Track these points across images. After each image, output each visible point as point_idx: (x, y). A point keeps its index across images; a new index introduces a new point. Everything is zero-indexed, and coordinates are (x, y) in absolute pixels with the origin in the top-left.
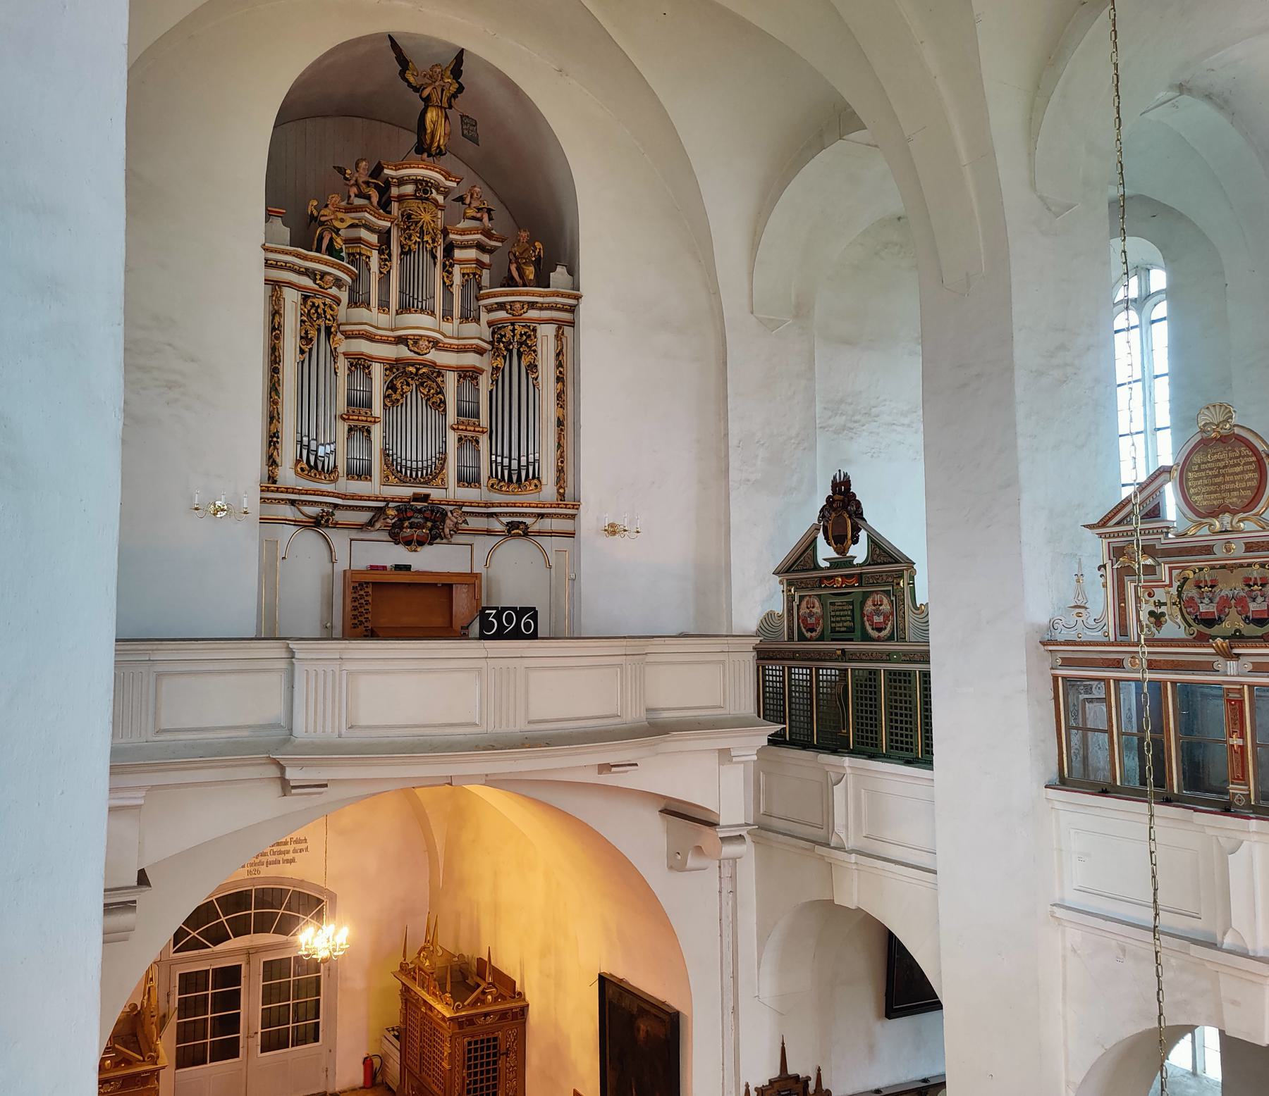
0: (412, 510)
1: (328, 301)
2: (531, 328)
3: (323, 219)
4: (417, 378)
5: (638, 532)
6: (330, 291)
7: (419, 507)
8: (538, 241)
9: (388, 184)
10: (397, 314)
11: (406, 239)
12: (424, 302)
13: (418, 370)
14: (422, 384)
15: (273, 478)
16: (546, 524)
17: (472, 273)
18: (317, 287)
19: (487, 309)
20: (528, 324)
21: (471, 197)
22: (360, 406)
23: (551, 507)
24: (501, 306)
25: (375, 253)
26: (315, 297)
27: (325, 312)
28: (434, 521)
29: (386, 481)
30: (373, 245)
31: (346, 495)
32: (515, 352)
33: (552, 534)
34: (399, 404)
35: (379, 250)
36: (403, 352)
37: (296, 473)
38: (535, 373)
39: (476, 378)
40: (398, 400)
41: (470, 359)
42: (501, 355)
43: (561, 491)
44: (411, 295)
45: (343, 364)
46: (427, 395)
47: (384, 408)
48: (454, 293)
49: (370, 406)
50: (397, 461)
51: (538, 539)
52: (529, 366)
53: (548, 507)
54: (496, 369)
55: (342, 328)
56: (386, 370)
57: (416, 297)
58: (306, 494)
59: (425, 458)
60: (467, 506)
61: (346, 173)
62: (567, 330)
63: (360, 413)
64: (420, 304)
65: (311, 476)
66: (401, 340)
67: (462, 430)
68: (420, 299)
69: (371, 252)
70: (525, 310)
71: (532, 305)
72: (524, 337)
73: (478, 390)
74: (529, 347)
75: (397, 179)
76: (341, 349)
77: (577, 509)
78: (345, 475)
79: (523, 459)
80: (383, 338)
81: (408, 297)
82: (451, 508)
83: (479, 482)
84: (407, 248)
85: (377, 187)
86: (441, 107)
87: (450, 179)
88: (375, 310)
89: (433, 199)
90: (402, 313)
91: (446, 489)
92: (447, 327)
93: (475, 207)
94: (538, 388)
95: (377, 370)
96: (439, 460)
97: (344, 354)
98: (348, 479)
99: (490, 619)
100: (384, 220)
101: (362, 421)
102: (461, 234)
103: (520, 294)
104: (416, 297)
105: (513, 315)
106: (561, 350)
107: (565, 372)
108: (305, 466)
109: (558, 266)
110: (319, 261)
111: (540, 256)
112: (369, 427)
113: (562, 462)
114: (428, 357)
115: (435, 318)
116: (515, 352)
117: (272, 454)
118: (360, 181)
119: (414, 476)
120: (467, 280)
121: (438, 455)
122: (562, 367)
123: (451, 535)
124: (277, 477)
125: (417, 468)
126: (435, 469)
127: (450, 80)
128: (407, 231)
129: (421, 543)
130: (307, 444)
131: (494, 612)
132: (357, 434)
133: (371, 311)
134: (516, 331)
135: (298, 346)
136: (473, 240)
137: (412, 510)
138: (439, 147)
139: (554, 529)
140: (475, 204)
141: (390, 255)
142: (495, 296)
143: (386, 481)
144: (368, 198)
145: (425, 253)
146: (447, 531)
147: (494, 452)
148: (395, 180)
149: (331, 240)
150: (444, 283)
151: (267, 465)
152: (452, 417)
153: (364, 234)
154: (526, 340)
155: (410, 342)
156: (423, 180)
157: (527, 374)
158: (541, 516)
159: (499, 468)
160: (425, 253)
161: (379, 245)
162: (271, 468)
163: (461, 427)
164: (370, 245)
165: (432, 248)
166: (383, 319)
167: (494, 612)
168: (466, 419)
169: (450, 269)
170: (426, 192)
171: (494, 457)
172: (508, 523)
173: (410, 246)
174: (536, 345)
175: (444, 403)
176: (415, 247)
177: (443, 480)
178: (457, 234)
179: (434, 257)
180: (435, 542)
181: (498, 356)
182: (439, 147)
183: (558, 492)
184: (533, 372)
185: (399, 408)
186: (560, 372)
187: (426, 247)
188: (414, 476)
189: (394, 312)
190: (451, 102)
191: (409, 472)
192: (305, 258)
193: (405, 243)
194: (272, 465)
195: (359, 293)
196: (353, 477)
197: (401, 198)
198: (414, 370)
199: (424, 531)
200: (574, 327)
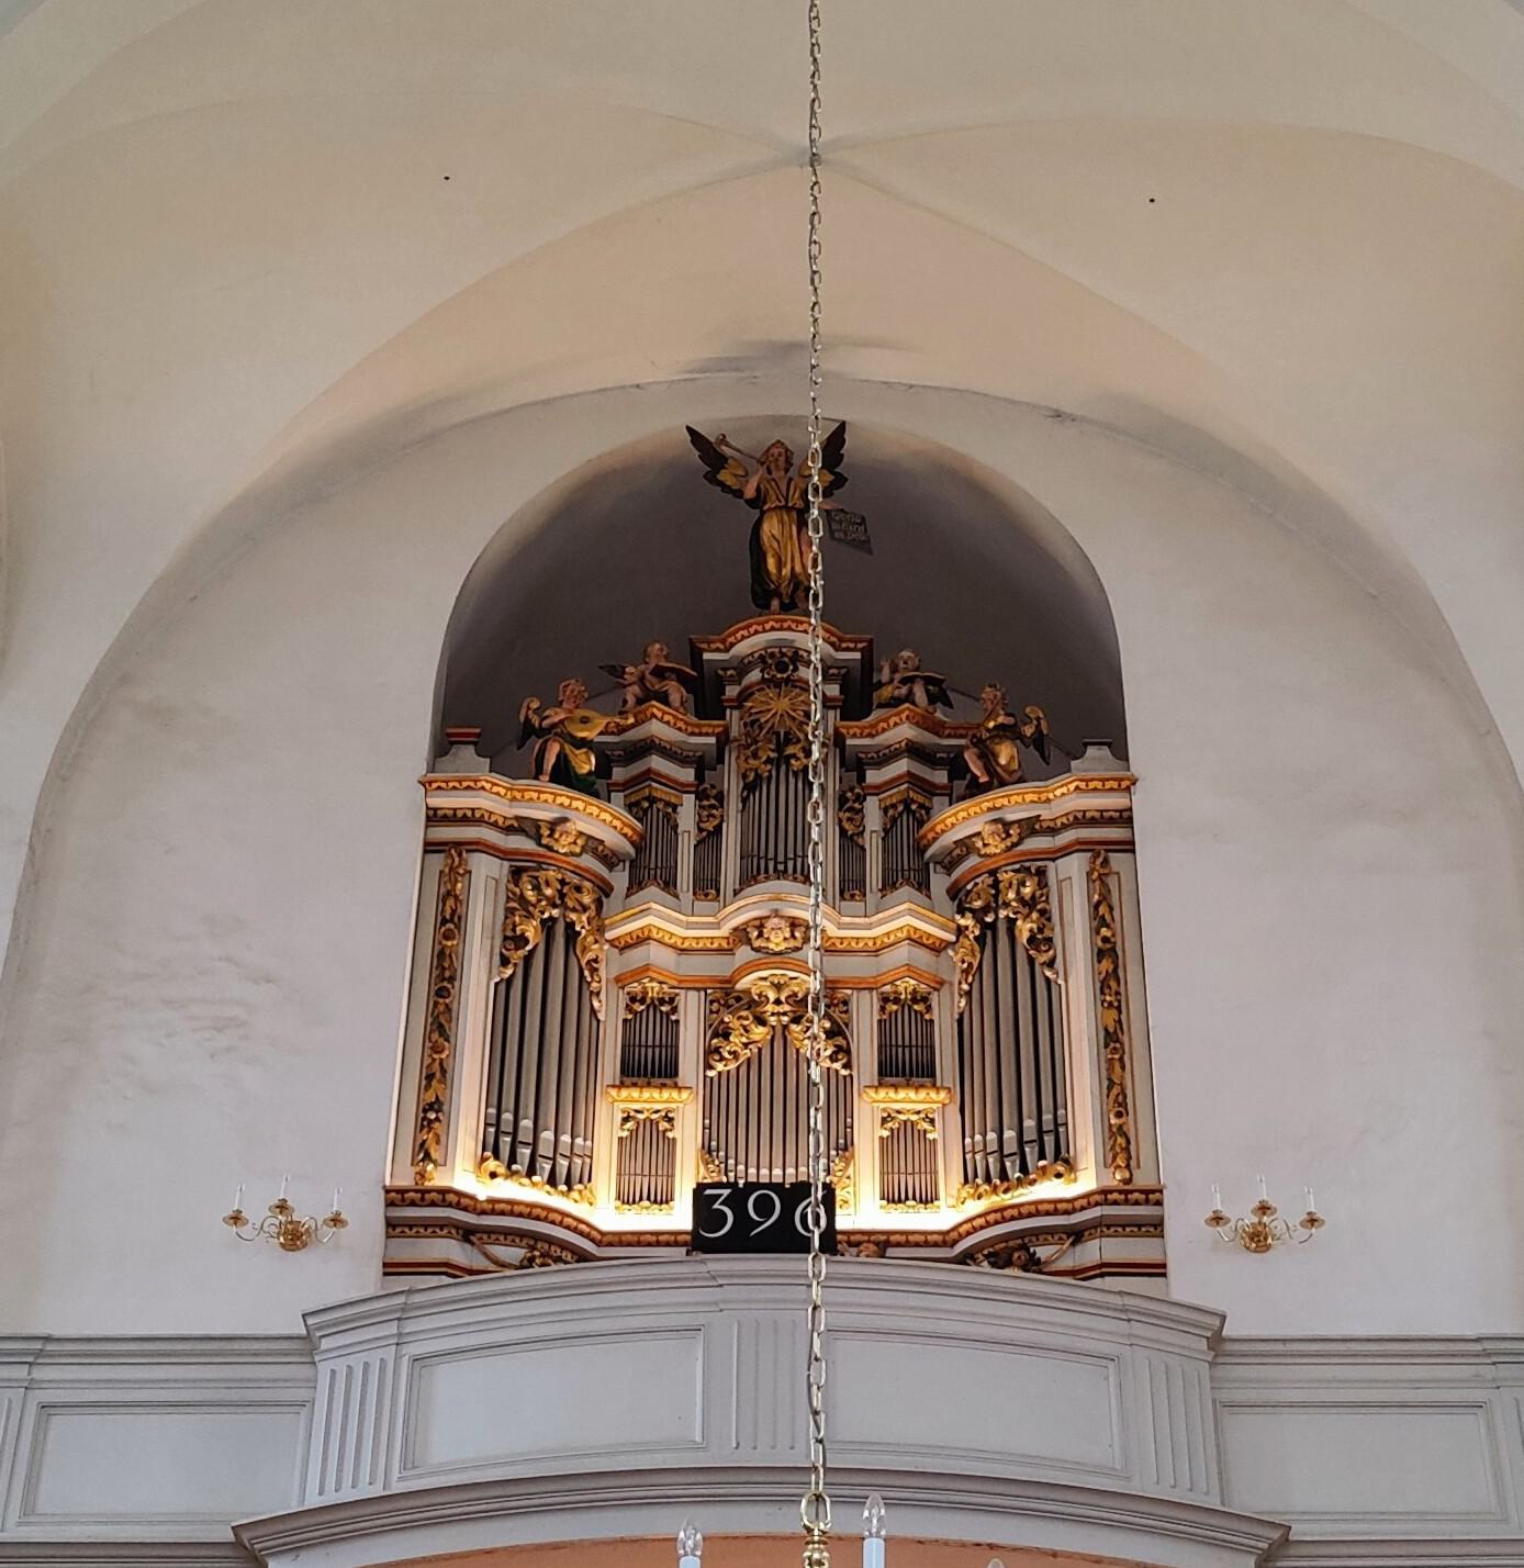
2: (1033, 871)
8: (1027, 705)
12: (790, 864)
17: (900, 802)
20: (1027, 864)
22: (645, 1075)
25: (689, 800)
30: (683, 785)
57: (771, 855)
60: (898, 1245)
64: (781, 867)
75: (734, 669)
79: (1029, 1123)
87: (844, 645)
89: (800, 680)
104: (771, 855)
109: (1089, 747)
111: (1041, 732)
133: (677, 897)
134: (1001, 885)
135: (497, 951)
141: (720, 798)
148: (729, 673)
150: (843, 832)
158: (1077, 1235)
164: (682, 788)
169: (857, 805)
174: (1047, 901)
175: (848, 1052)
178: (862, 736)
197: (745, 695)
200: (1133, 851)
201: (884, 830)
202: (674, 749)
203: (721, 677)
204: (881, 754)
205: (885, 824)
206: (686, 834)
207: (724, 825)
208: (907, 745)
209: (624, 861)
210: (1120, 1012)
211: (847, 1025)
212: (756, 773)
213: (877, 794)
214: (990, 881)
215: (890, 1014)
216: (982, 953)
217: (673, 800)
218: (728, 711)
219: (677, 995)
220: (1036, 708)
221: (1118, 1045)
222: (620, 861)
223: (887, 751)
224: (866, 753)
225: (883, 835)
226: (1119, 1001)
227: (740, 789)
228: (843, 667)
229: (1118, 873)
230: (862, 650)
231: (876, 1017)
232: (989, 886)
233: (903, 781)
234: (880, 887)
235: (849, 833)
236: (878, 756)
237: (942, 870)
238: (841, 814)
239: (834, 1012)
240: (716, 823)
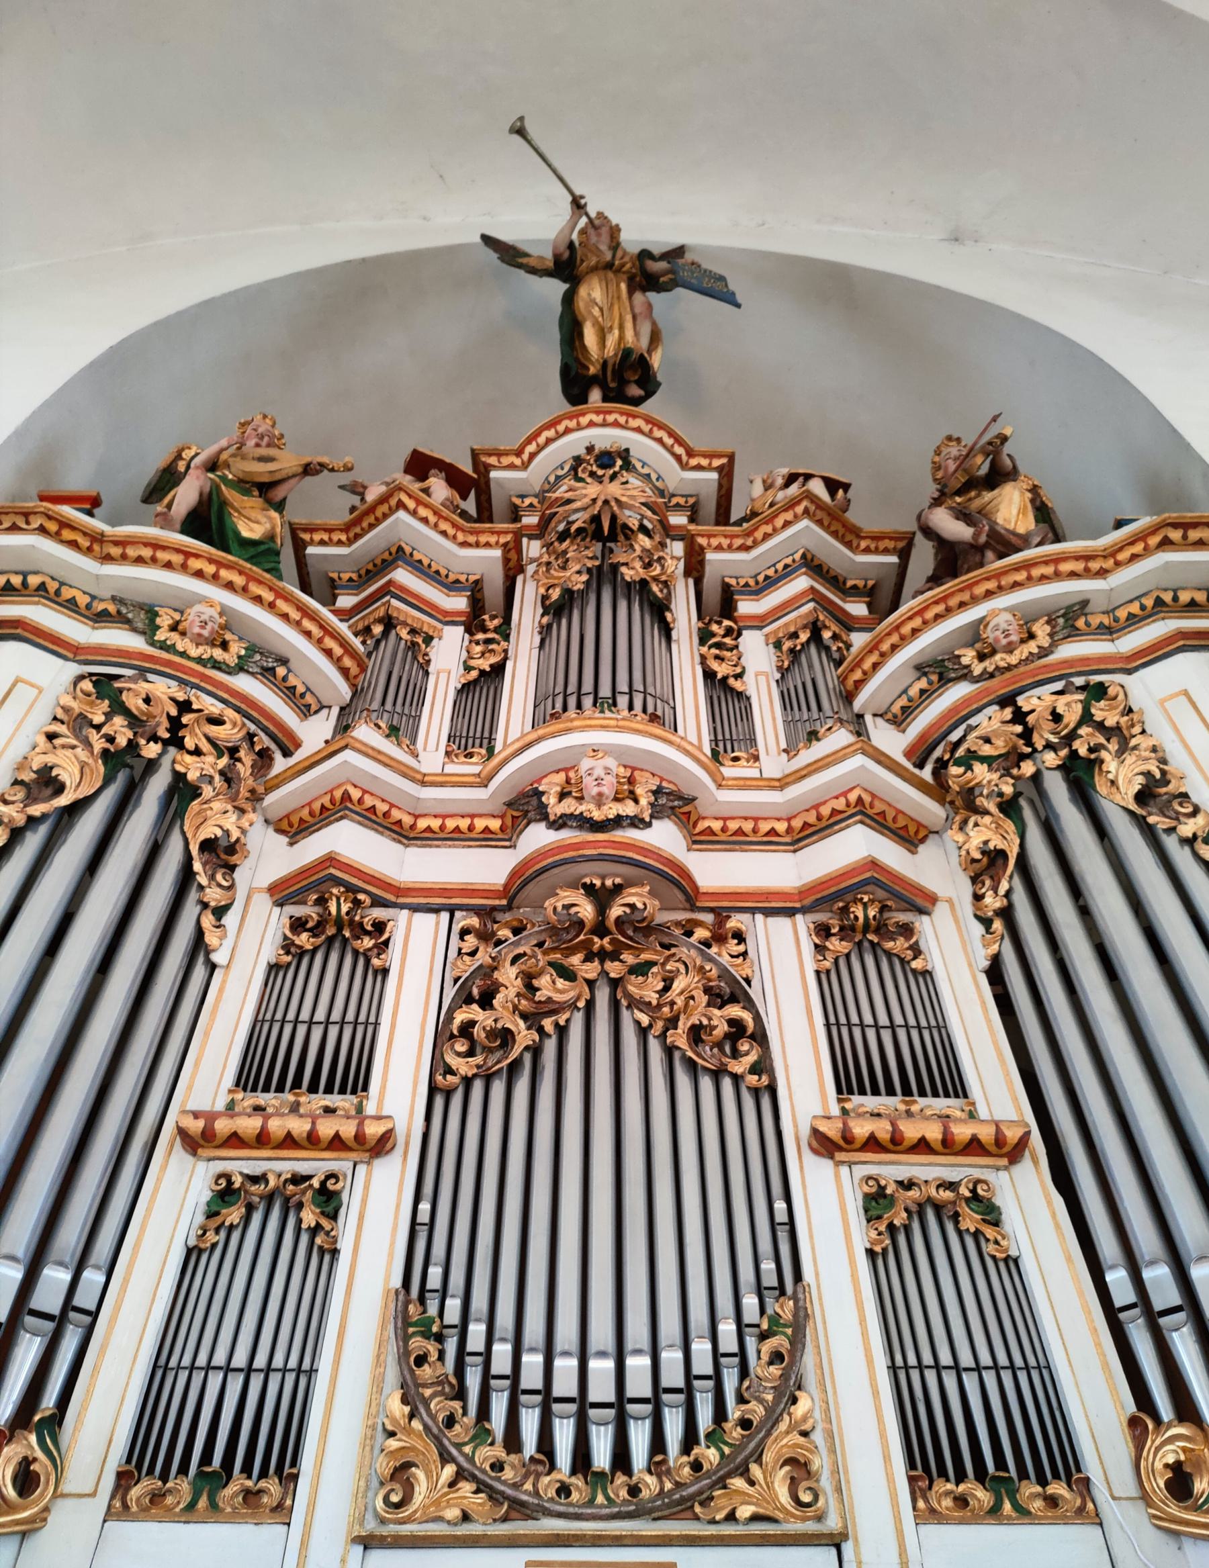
13: (602, 897)
73: (927, 974)
91: (836, 1542)
100: (477, 545)
119: (602, 1457)
125: (621, 1401)
150: (709, 675)
157: (1150, 834)
169: (728, 640)
171: (1117, 1278)
177: (799, 1468)
179: (659, 611)
188: (602, 1457)
191: (564, 1435)
201: (779, 668)
209: (330, 707)
211: (748, 981)
213: (760, 628)
215: (836, 960)
222: (322, 707)
225: (778, 676)
230: (720, 469)
231: (810, 968)
234: (783, 745)
236: (757, 583)
238: (704, 649)
239: (720, 955)
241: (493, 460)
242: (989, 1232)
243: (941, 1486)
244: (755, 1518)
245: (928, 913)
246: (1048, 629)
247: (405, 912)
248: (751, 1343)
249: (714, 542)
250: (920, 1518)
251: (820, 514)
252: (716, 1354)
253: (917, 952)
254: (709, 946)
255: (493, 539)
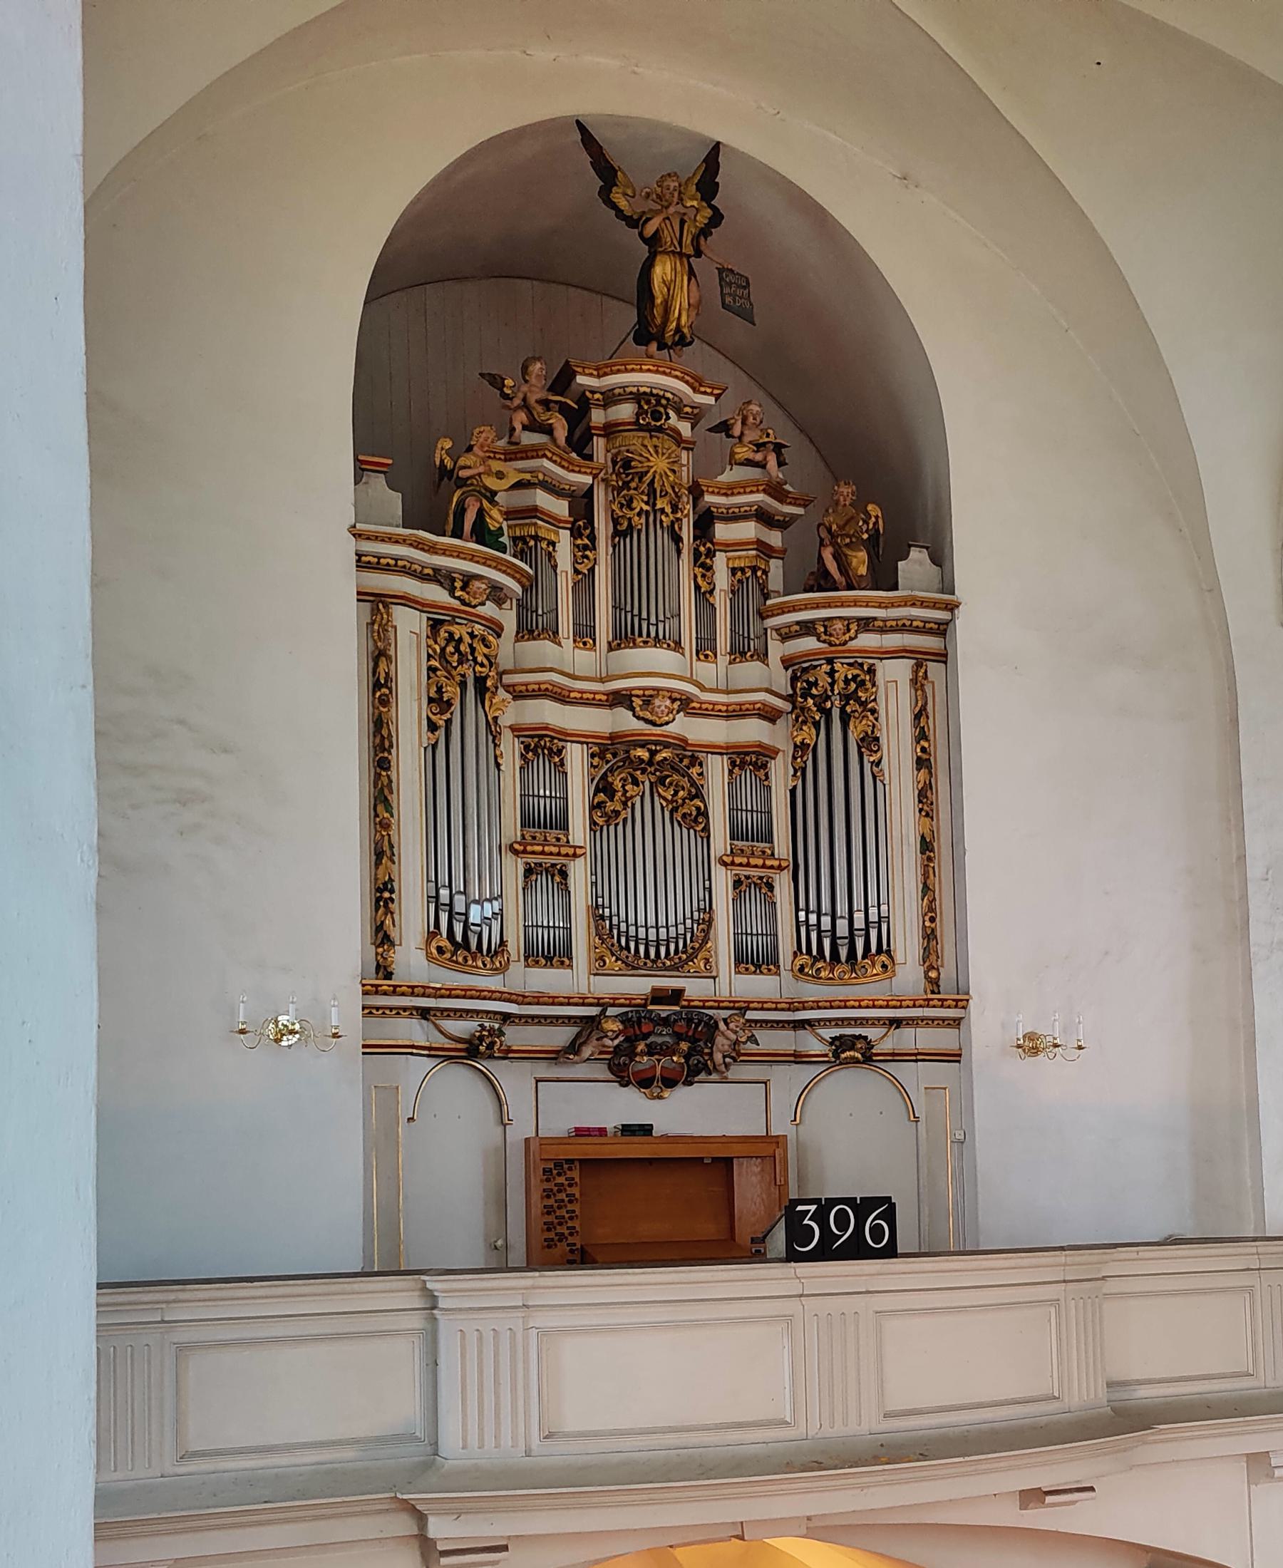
0: (651, 1020)
1: (478, 629)
2: (866, 668)
3: (463, 474)
4: (653, 769)
5: (1080, 1048)
6: (481, 610)
7: (664, 1015)
8: (873, 503)
9: (584, 404)
10: (610, 649)
11: (622, 506)
12: (661, 626)
13: (653, 753)
14: (662, 781)
15: (385, 968)
16: (907, 1039)
18: (456, 603)
19: (780, 635)
20: (860, 660)
21: (744, 423)
22: (545, 827)
23: (914, 1006)
24: (807, 628)
25: (565, 535)
26: (452, 623)
27: (473, 650)
28: (693, 1040)
29: (599, 967)
30: (560, 521)
31: (524, 997)
32: (836, 713)
33: (917, 1057)
34: (620, 820)
35: (571, 530)
36: (624, 721)
37: (429, 957)
38: (876, 752)
39: (764, 766)
40: (617, 813)
41: (752, 731)
42: (810, 720)
43: (933, 974)
44: (636, 612)
45: (510, 748)
46: (672, 802)
47: (591, 829)
48: (717, 606)
49: (564, 826)
50: (619, 929)
51: (891, 1067)
52: (863, 740)
53: (908, 1007)
54: (801, 748)
55: (507, 679)
56: (593, 756)
57: (644, 615)
58: (449, 996)
59: (672, 921)
60: (755, 1009)
61: (504, 385)
62: (934, 669)
63: (546, 840)
64: (653, 629)
65: (456, 962)
66: (619, 699)
67: (741, 865)
68: (653, 620)
69: (557, 534)
70: (852, 633)
71: (866, 625)
72: (853, 686)
74: (863, 704)
75: (602, 393)
76: (507, 720)
77: (963, 1007)
78: (522, 958)
79: (859, 917)
80: (585, 696)
81: (629, 616)
82: (725, 1014)
83: (776, 963)
84: (626, 524)
85: (564, 409)
86: (681, 254)
87: (702, 389)
88: (568, 643)
90: (619, 647)
91: (714, 978)
92: (706, 671)
93: (750, 442)
94: (882, 781)
95: (576, 757)
96: (699, 924)
97: (513, 729)
98: (527, 966)
99: (806, 1222)
100: (579, 472)
101: (551, 854)
102: (726, 495)
103: (843, 604)
105: (831, 644)
106: (924, 708)
107: (932, 748)
108: (445, 943)
109: (912, 548)
110: (459, 554)
112: (564, 865)
113: (932, 920)
114: (670, 728)
115: (683, 654)
116: (836, 713)
117: (382, 923)
118: (532, 399)
119: (652, 955)
120: (740, 581)
121: (696, 915)
122: (927, 739)
123: (727, 1066)
124: (393, 966)
125: (658, 940)
126: (691, 941)
127: (695, 203)
128: (625, 492)
129: (670, 1083)
130: (448, 902)
131: (813, 1208)
132: (542, 880)
133: (559, 644)
134: (837, 675)
135: (424, 716)
136: (750, 505)
137: (651, 1020)
138: (678, 329)
139: (921, 1046)
140: (751, 435)
141: (592, 538)
142: (794, 608)
143: (599, 967)
144: (549, 430)
145: (659, 532)
146: (718, 1057)
147: (802, 904)
148: (597, 396)
149: (481, 513)
150: (697, 587)
151: (373, 944)
152: (720, 841)
153: (542, 499)
154: (856, 690)
155: (637, 702)
156: (652, 394)
158: (896, 1023)
159: (814, 936)
160: (659, 532)
161: (571, 519)
162: (380, 950)
163: (738, 860)
164: (554, 521)
165: (673, 523)
166: (584, 660)
167: (813, 1208)
168: (745, 843)
169: (708, 561)
170: (656, 416)
172: (834, 1039)
173: (630, 519)
174: (875, 700)
175: (704, 813)
176: (639, 522)
177: (707, 961)
178: (718, 493)
179: (677, 539)
180: (696, 1079)
181: (804, 722)
182: (678, 329)
183: (927, 977)
184: (871, 751)
185: (620, 827)
186: (923, 750)
187: (661, 521)
188: (652, 955)
189: (605, 646)
190: (698, 243)
191: (642, 948)
192: (432, 549)
193: (621, 514)
194: (382, 944)
195: (537, 611)
196: (537, 962)
197: (610, 430)
198: (642, 753)
199: (675, 1059)
200: (945, 663)
202: (553, 483)
203: (589, 399)
204: (731, 511)
205: (732, 585)
206: (564, 574)
207: (597, 567)
208: (756, 510)
210: (933, 820)
211: (702, 786)
212: (630, 525)
213: (726, 551)
214: (826, 668)
216: (818, 735)
217: (553, 538)
218: (595, 438)
219: (563, 747)
220: (879, 510)
221: (932, 854)
223: (737, 510)
224: (717, 508)
226: (932, 810)
227: (610, 535)
228: (696, 408)
229: (933, 683)
232: (826, 673)
233: (751, 547)
234: (728, 651)
235: (703, 590)
236: (728, 513)
237: (779, 638)
240: (589, 567)
241: (579, 370)
242: (769, 894)
243: (742, 965)
244: (695, 972)
245: (774, 759)
246: (856, 628)
247: (569, 744)
248: (695, 926)
249: (710, 490)
250: (736, 973)
251: (771, 490)
252: (685, 928)
253: (767, 778)
254: (689, 769)
255: (589, 471)
